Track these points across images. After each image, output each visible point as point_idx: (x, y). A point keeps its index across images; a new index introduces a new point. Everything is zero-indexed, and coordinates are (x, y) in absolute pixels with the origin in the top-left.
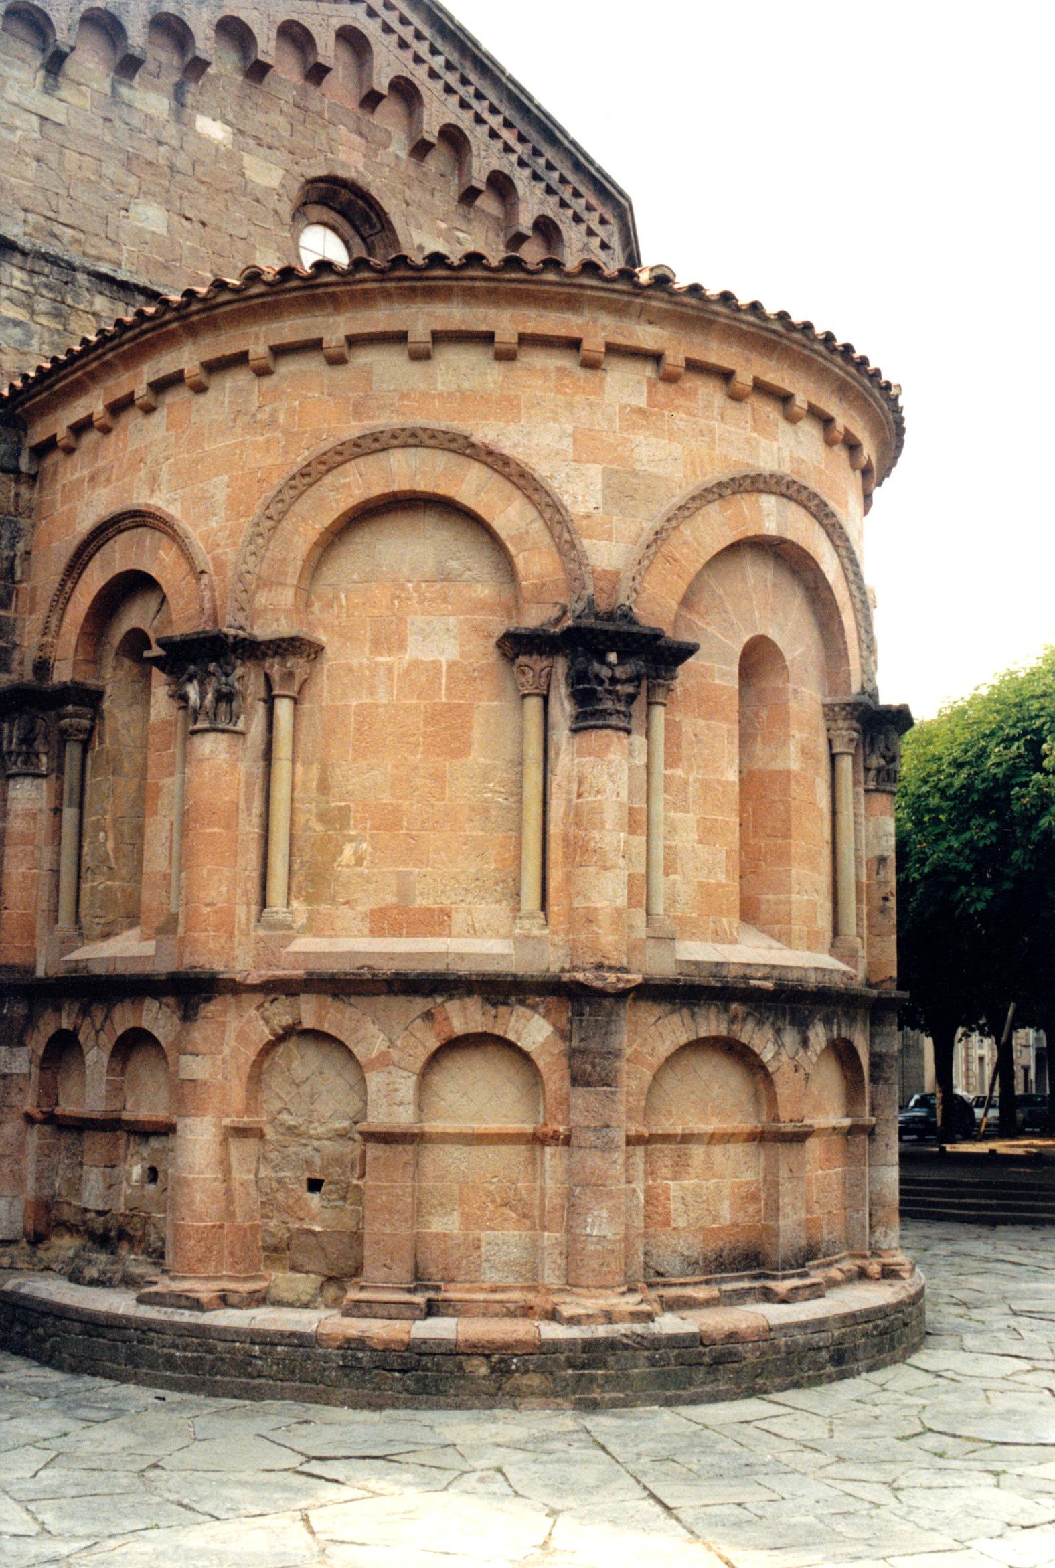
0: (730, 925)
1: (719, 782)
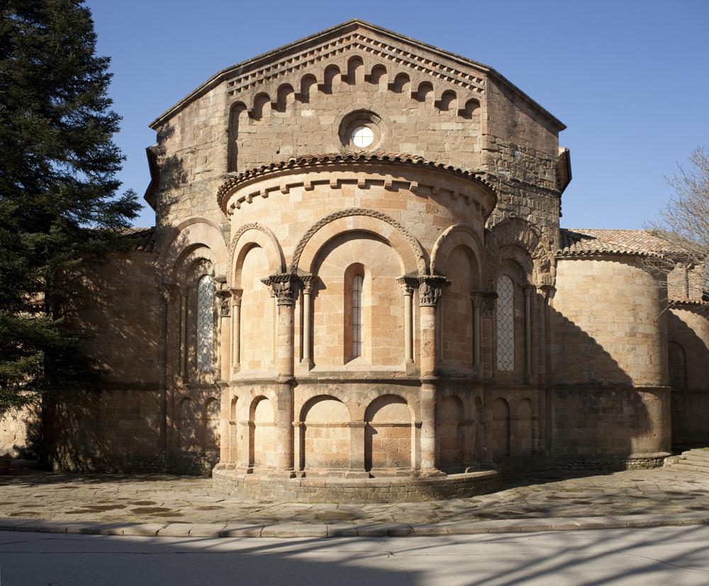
0: (340, 359)
1: (335, 314)
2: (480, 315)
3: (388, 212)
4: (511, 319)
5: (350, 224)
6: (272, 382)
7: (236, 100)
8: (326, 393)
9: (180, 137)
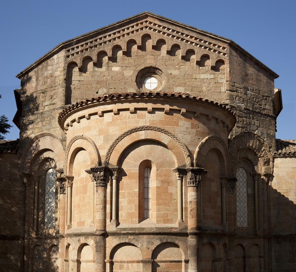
0: (136, 220)
1: (133, 192)
2: (226, 192)
3: (167, 128)
4: (245, 195)
5: (142, 135)
6: (92, 235)
7: (71, 61)
8: (127, 241)
9: (36, 83)
